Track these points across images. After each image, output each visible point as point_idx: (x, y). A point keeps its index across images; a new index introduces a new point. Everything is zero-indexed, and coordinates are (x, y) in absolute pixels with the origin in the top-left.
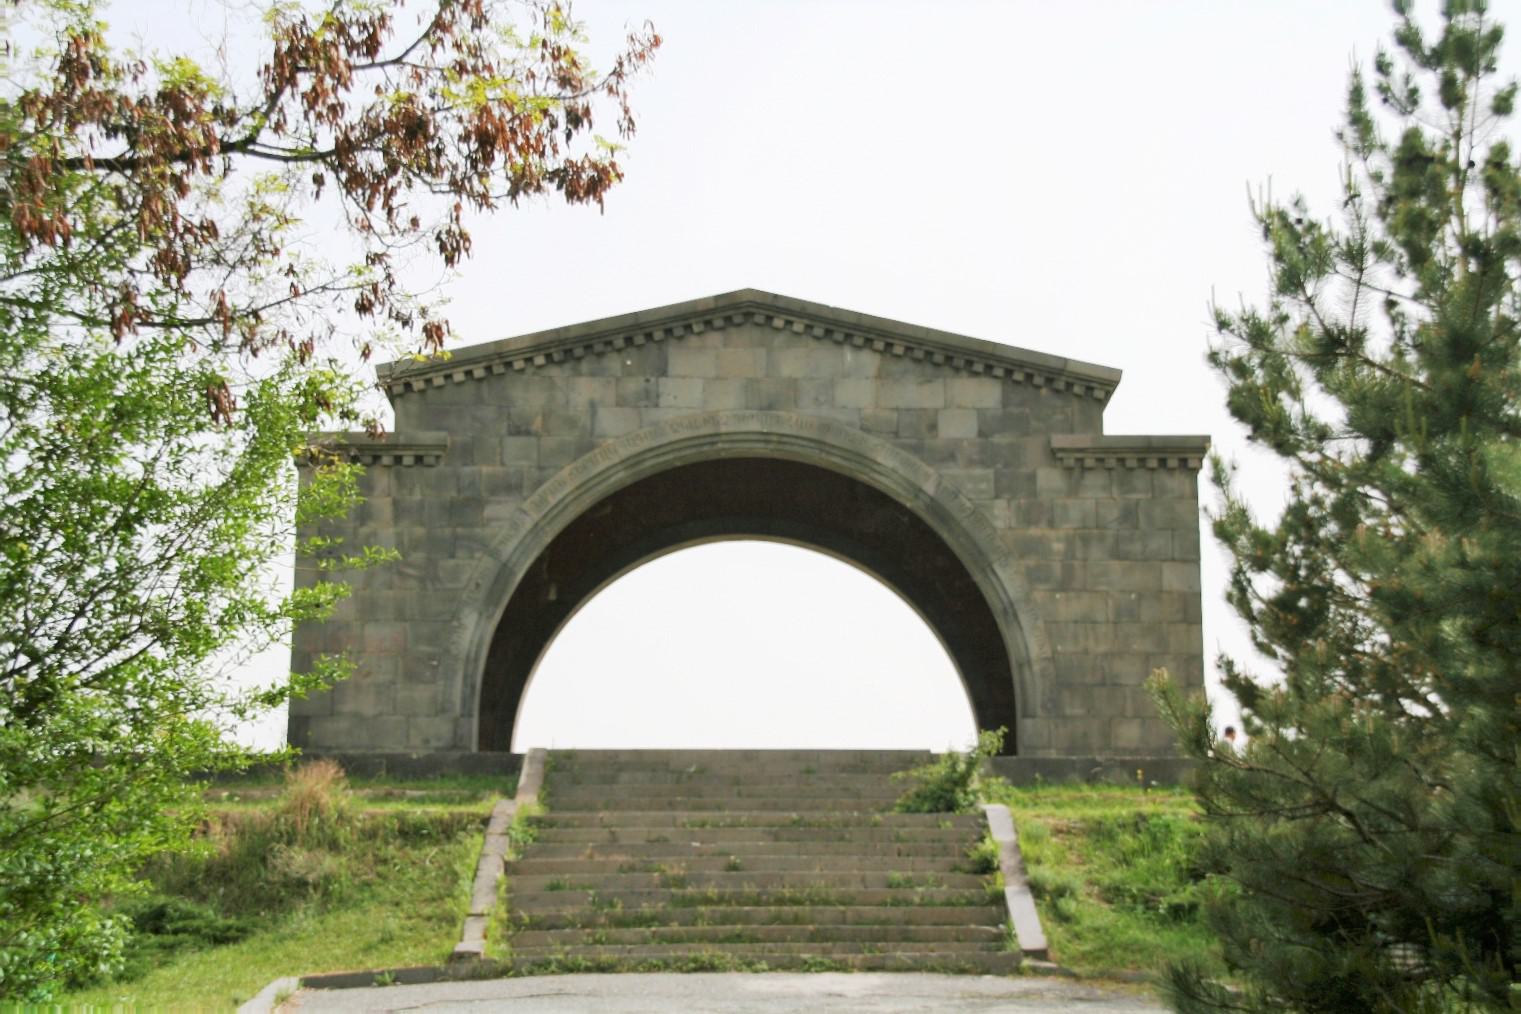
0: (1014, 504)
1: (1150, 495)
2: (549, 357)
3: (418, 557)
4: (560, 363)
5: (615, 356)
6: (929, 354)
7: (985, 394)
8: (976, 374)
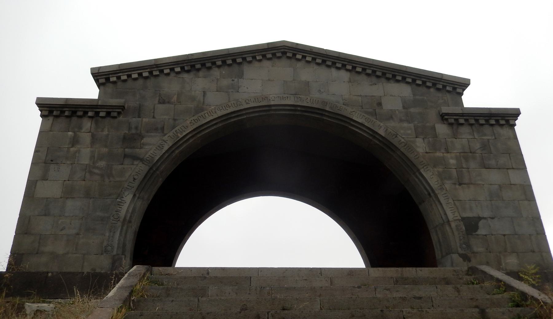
0: (426, 140)
1: (494, 138)
2: (182, 68)
4: (188, 71)
5: (216, 69)
6: (374, 72)
7: (405, 91)
8: (398, 81)
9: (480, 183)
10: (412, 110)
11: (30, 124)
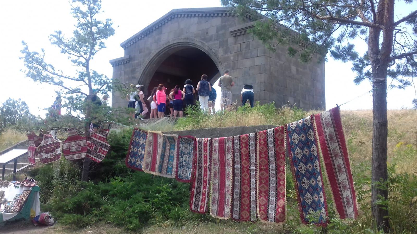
7: (217, 22)
9: (241, 67)
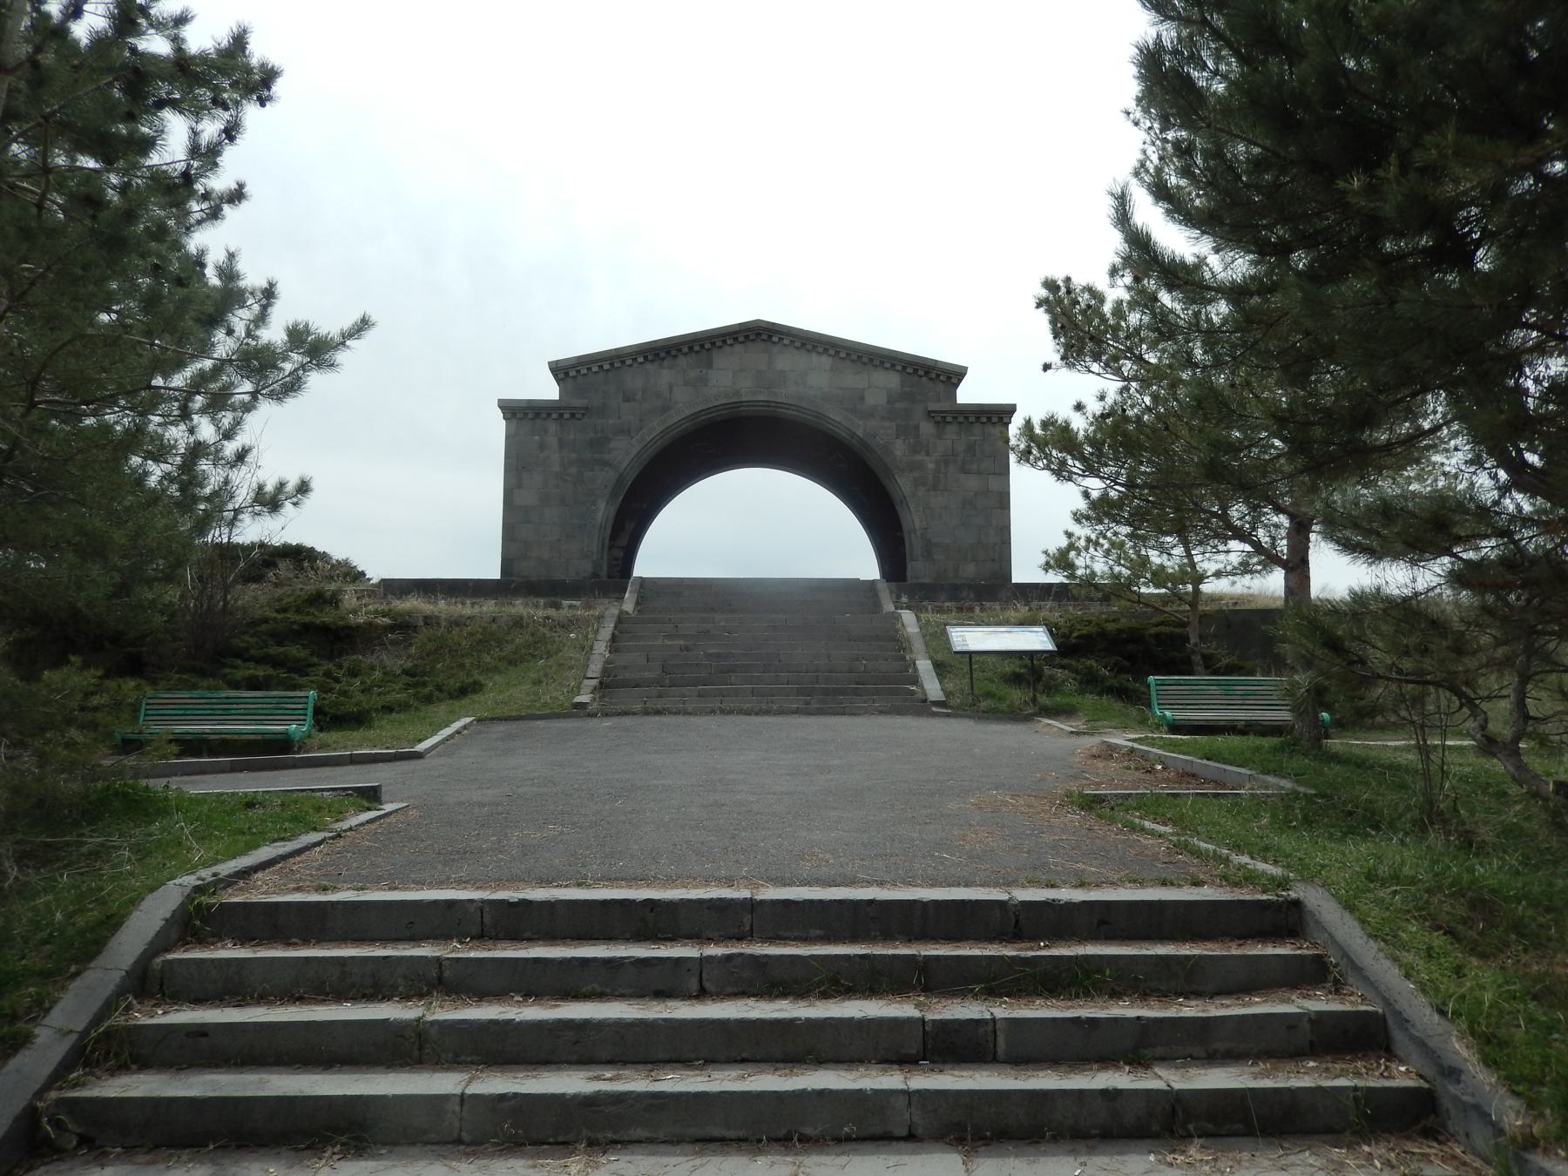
2: (646, 358)
3: (573, 470)
7: (891, 380)
10: (898, 405)
11: (496, 429)
